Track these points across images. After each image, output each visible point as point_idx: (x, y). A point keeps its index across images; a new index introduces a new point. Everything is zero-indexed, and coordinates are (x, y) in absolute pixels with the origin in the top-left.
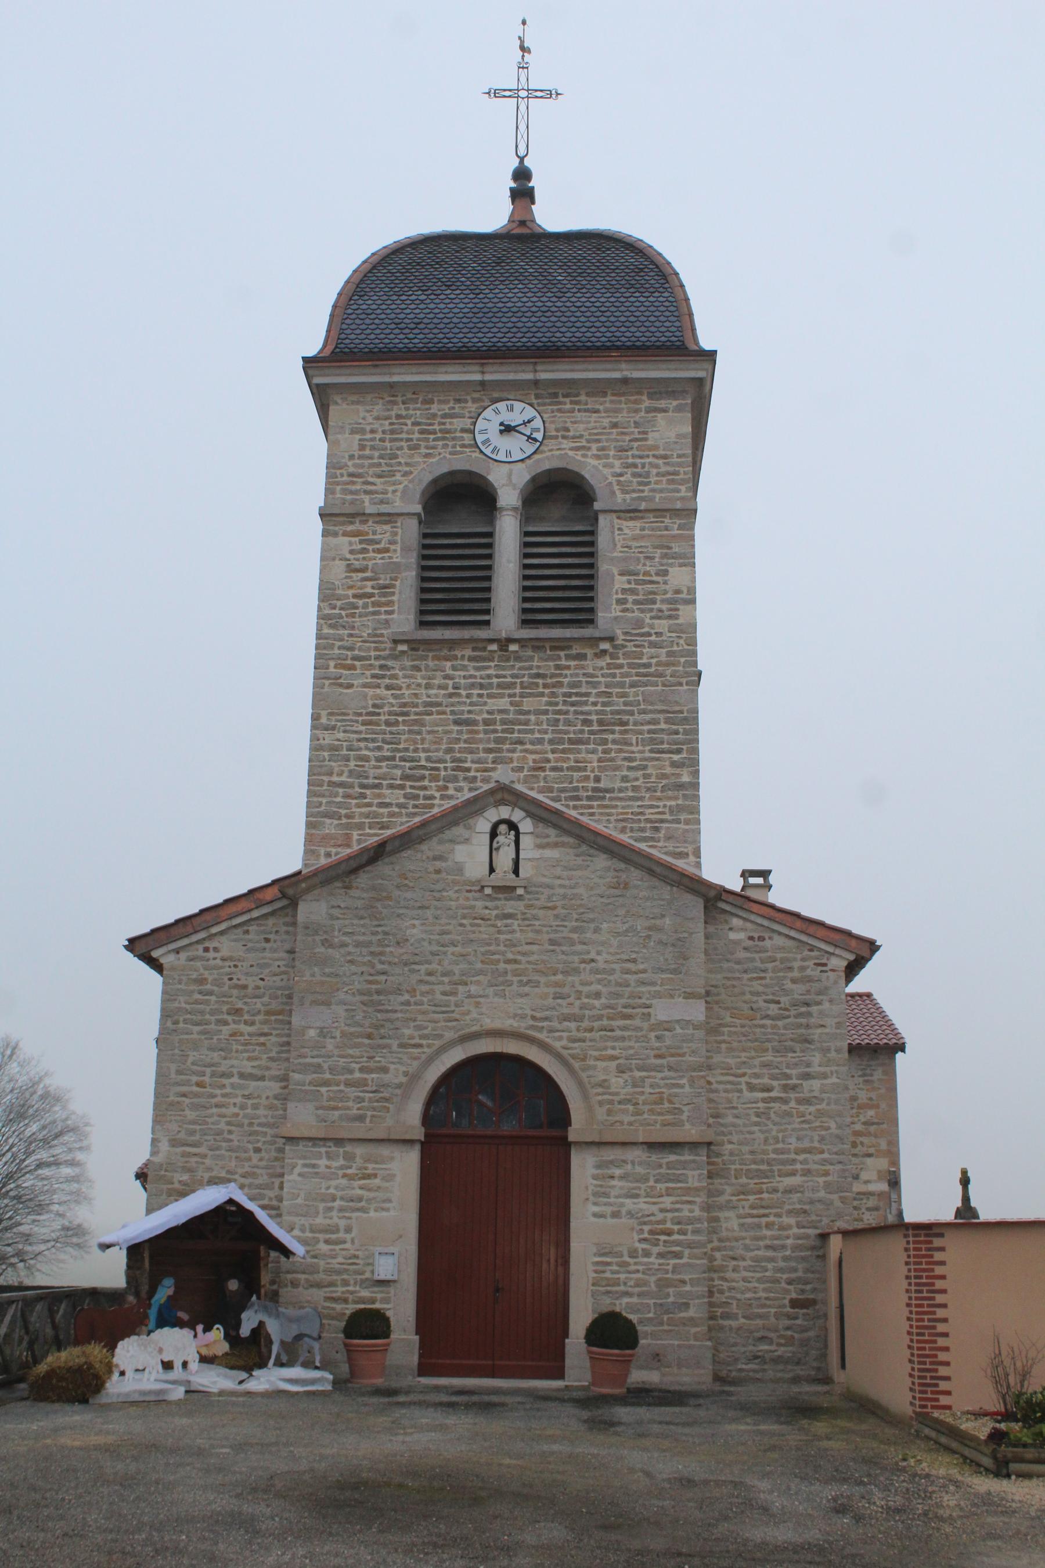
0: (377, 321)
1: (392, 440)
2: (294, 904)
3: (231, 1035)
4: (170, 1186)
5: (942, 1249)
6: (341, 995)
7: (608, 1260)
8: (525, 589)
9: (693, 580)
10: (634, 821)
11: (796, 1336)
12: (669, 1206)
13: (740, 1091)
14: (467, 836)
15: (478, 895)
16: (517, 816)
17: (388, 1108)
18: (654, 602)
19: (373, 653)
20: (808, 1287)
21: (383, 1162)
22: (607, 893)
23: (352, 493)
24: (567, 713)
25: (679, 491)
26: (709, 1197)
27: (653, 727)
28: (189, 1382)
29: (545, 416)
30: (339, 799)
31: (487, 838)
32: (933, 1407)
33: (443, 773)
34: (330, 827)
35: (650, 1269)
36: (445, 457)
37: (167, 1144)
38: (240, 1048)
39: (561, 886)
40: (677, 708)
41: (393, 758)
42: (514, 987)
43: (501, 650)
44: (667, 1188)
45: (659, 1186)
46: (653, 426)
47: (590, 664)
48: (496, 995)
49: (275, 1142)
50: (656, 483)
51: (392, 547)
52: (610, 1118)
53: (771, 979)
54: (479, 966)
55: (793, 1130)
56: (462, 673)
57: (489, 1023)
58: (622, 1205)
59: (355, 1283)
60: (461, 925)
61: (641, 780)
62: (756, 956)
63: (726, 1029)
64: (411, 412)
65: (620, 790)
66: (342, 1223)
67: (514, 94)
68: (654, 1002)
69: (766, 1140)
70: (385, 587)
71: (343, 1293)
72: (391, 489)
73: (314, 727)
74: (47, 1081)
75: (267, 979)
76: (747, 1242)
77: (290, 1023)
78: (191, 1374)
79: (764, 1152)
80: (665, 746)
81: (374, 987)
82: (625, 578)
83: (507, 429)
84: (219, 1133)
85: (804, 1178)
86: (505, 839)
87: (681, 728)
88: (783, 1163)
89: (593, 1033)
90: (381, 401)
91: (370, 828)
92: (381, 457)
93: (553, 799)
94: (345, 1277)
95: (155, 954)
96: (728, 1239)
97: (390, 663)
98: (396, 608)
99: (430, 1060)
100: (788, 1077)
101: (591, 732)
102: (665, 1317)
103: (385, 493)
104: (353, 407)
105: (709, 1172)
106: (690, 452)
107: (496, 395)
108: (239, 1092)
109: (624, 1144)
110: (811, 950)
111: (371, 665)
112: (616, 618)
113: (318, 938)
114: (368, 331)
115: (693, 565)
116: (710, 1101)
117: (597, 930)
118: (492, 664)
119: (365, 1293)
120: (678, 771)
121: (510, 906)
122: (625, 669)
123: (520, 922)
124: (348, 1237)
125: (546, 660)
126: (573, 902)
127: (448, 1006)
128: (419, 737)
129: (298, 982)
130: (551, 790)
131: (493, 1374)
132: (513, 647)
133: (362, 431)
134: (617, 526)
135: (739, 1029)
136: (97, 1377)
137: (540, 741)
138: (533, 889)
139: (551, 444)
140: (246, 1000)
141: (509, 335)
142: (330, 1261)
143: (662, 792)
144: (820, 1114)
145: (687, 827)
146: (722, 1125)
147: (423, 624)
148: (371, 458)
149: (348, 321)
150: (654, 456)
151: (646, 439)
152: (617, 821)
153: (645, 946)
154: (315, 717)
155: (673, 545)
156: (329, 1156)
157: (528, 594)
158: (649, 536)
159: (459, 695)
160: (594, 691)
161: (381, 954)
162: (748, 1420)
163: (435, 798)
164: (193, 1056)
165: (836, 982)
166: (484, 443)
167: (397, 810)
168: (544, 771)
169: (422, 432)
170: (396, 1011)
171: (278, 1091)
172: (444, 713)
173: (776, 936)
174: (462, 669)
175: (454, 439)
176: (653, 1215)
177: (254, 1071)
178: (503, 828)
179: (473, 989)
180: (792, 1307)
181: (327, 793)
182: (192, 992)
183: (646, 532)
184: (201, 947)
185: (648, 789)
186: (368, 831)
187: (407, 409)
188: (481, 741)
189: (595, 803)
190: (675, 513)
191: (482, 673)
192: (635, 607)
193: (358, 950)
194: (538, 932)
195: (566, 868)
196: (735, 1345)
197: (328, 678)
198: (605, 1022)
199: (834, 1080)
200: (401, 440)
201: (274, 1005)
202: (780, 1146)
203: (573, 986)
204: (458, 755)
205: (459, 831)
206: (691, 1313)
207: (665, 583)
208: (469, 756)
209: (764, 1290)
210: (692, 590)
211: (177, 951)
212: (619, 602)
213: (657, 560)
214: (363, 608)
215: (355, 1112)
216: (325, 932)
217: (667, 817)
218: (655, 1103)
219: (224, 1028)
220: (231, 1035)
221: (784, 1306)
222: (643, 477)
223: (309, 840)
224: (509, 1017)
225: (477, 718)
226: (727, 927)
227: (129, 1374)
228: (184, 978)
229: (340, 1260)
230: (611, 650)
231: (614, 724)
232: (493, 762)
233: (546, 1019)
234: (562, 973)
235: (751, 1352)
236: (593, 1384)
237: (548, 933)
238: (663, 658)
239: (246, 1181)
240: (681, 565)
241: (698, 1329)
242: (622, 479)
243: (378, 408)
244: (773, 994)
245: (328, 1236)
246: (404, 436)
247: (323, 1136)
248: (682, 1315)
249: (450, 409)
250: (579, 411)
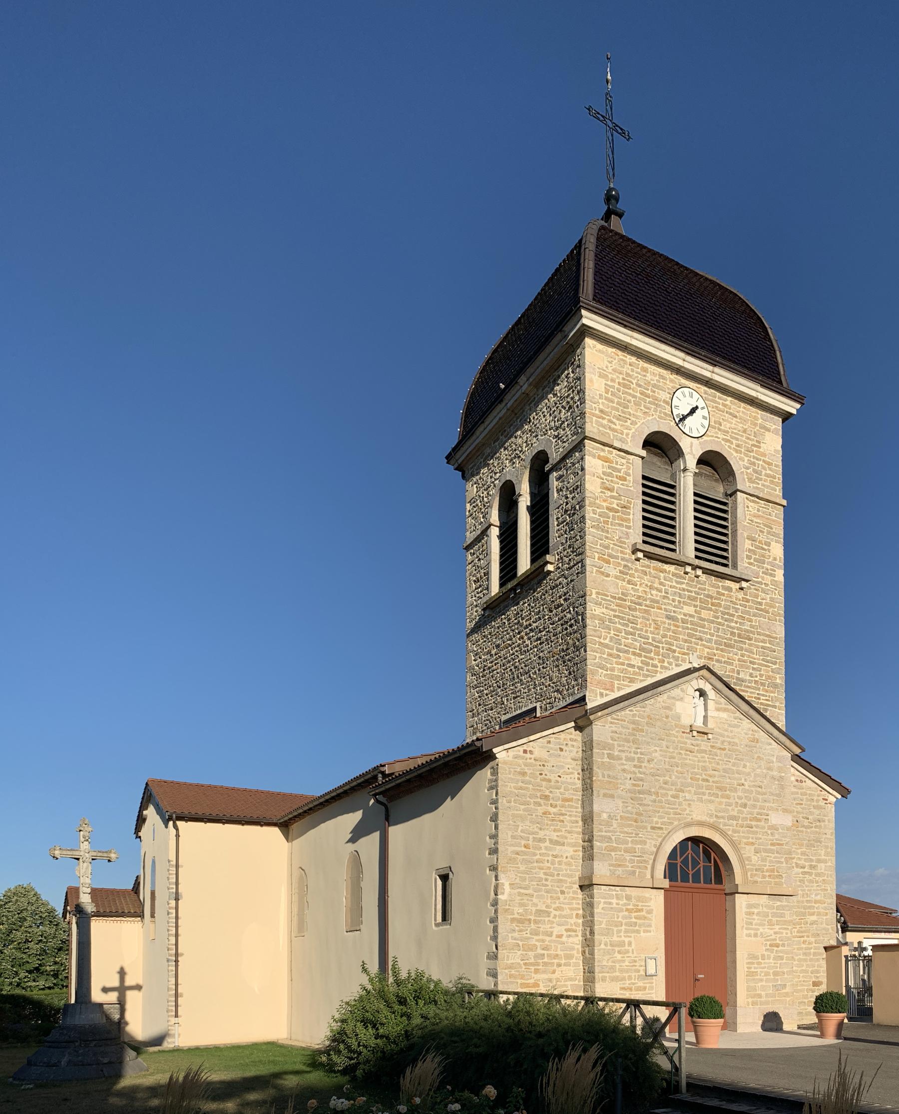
12: (777, 930)
30: (605, 656)
60: (680, 753)
84: (540, 879)
108: (551, 853)
124: (630, 949)
137: (710, 641)
156: (618, 898)
161: (640, 767)
171: (572, 853)
172: (661, 609)
179: (688, 796)
184: (521, 749)
195: (730, 725)
199: (829, 864)
205: (676, 692)
229: (627, 964)
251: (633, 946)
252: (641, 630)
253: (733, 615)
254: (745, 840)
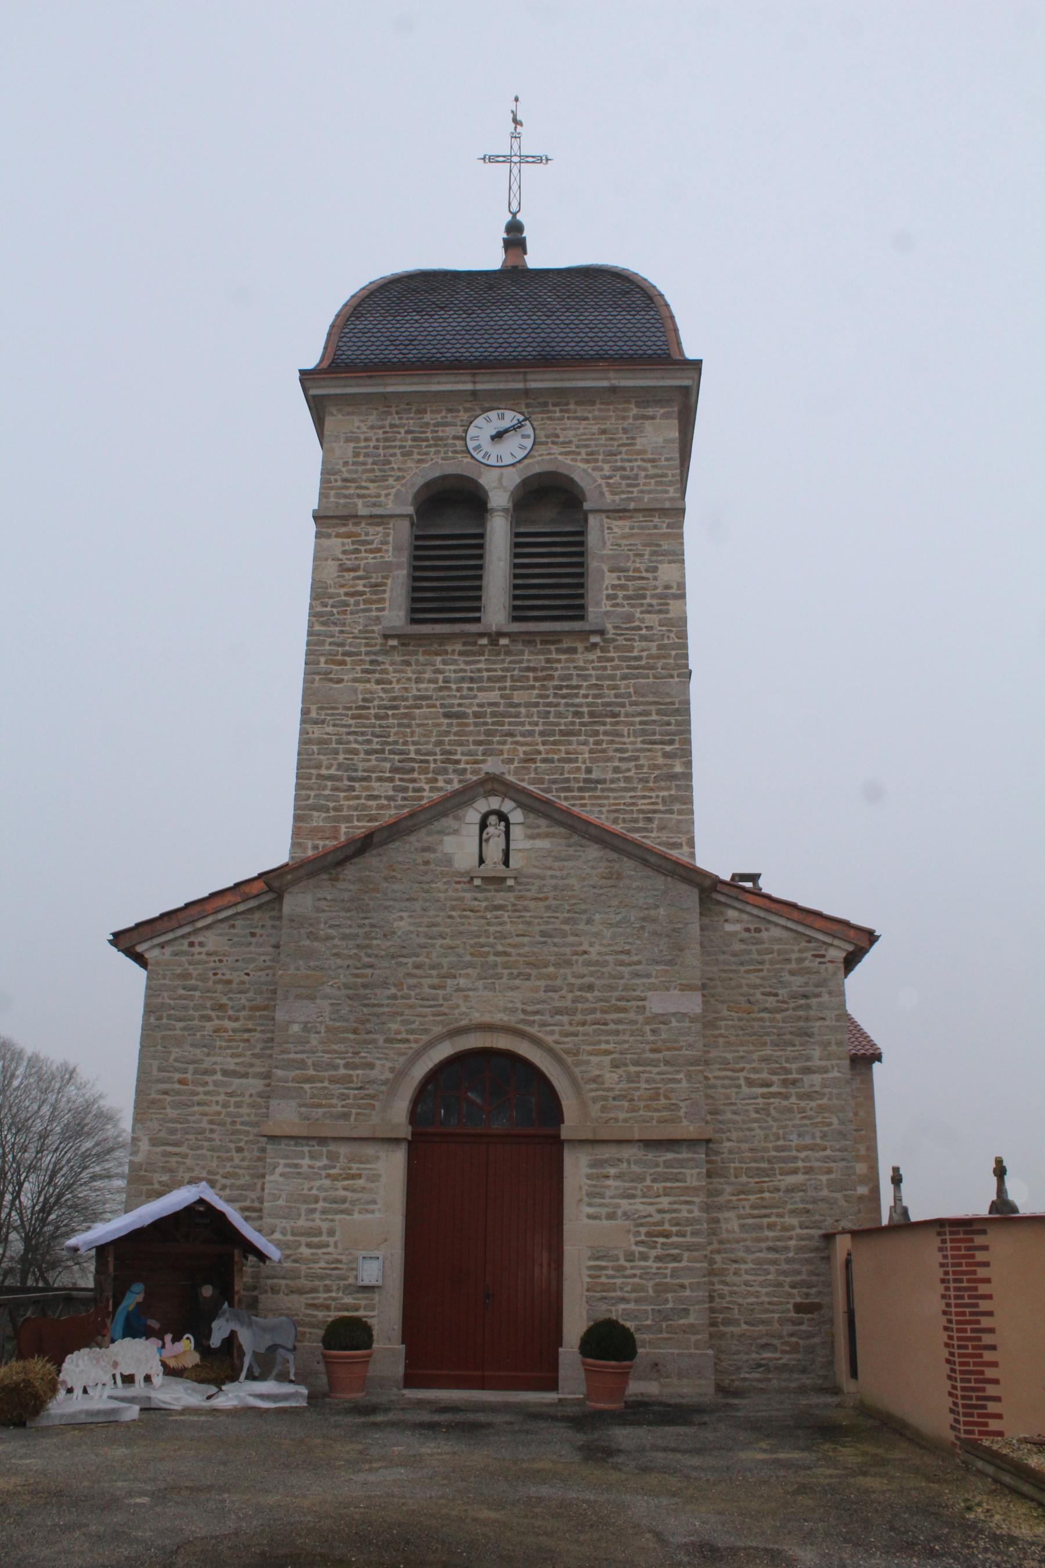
0: (373, 339)
1: (385, 448)
2: (280, 898)
3: (215, 1032)
4: (150, 1187)
5: (985, 1248)
6: (328, 990)
7: (604, 1264)
8: (516, 587)
9: (683, 576)
10: (625, 812)
11: (801, 1342)
12: (666, 1206)
13: (739, 1086)
14: (456, 827)
15: (467, 886)
16: (507, 806)
17: (374, 1106)
18: (644, 597)
19: (363, 649)
20: (813, 1290)
21: (368, 1162)
22: (600, 883)
23: (346, 497)
24: (557, 705)
25: (667, 492)
26: (708, 1197)
27: (645, 719)
28: (149, 1398)
29: (535, 423)
30: (327, 792)
31: (476, 829)
32: (981, 1433)
33: (432, 765)
34: (318, 819)
35: (648, 1273)
36: (437, 463)
37: (147, 1143)
38: (224, 1044)
39: (552, 877)
40: (669, 700)
41: (383, 751)
42: (504, 980)
43: (491, 645)
44: (665, 1188)
45: (656, 1185)
46: (642, 432)
47: (580, 658)
48: (485, 988)
49: (258, 1142)
50: (645, 484)
51: (384, 547)
52: (604, 1115)
53: (768, 970)
54: (468, 958)
55: (794, 1126)
56: (452, 667)
57: (477, 1017)
58: (618, 1206)
59: (338, 1289)
60: (450, 917)
61: (633, 771)
62: (754, 948)
63: (723, 1023)
64: (404, 421)
65: (612, 781)
66: (325, 1226)
67: (507, 159)
68: (649, 994)
69: (766, 1137)
70: (377, 585)
71: (325, 1299)
72: (383, 493)
73: (303, 721)
74: (102, 1103)
75: (252, 973)
76: (748, 1243)
77: (273, 1019)
78: (154, 1389)
79: (766, 1150)
80: (657, 737)
81: (360, 980)
82: (615, 575)
83: (498, 436)
84: (202, 1132)
85: (807, 1177)
86: (495, 829)
87: (672, 719)
88: (784, 1160)
89: (586, 1027)
90: (375, 412)
91: (358, 821)
92: (374, 463)
93: (543, 790)
94: (327, 1282)
95: (139, 949)
96: (729, 1241)
97: (380, 659)
98: (387, 605)
99: (418, 1054)
100: (788, 1071)
101: (582, 724)
102: (664, 1325)
103: (378, 496)
104: (349, 417)
105: (708, 1171)
106: (677, 455)
107: (487, 405)
109: (619, 1142)
110: (809, 942)
111: (361, 660)
112: (606, 613)
113: (303, 931)
114: (364, 348)
115: (683, 561)
116: (708, 1097)
117: (589, 922)
118: (482, 658)
119: (348, 1300)
120: (669, 762)
121: (500, 898)
122: (616, 662)
123: (510, 913)
124: (331, 1240)
125: (536, 654)
126: (565, 892)
127: (437, 1000)
128: (408, 730)
129: (282, 975)
130: (541, 781)
131: (482, 1384)
132: (504, 641)
133: (357, 440)
134: (606, 526)
135: (736, 1022)
136: (36, 1396)
137: (531, 733)
138: (525, 880)
139: (541, 449)
140: (230, 995)
141: (501, 350)
142: (311, 1265)
143: (654, 782)
144: (821, 1109)
145: (680, 817)
146: (721, 1122)
147: (414, 621)
148: (364, 464)
149: (345, 339)
150: (643, 460)
151: (634, 444)
152: (609, 811)
153: (638, 938)
154: (305, 712)
155: (662, 543)
156: (312, 1157)
157: (518, 592)
158: (639, 534)
159: (449, 689)
160: (585, 684)
161: (367, 946)
162: (763, 1445)
163: (424, 790)
164: (176, 1052)
165: (835, 974)
166: (475, 449)
167: (386, 802)
168: (535, 762)
169: (414, 440)
170: (382, 1005)
171: (261, 1088)
172: (434, 706)
173: (773, 928)
174: (452, 665)
175: (445, 445)
176: (650, 1216)
177: (237, 1068)
178: (493, 819)
179: (462, 982)
180: (797, 1312)
181: (316, 786)
182: (177, 987)
183: (636, 531)
184: (186, 942)
185: (641, 780)
186: (356, 823)
187: (400, 419)
188: (470, 733)
189: (587, 794)
190: (664, 512)
191: (472, 667)
192: (625, 602)
193: (344, 943)
194: (529, 923)
195: (556, 859)
196: (738, 1352)
197: (319, 674)
198: (598, 1015)
199: (835, 1074)
200: (395, 447)
201: (259, 1001)
202: (781, 1143)
203: (565, 979)
204: (448, 748)
205: (448, 822)
206: (692, 1319)
207: (655, 579)
208: (459, 748)
209: (767, 1294)
210: (682, 586)
211: (162, 946)
212: (609, 597)
213: (646, 557)
214: (355, 605)
215: (340, 1109)
216: (311, 925)
217: (660, 807)
218: (651, 1099)
219: (208, 1024)
220: (215, 1032)
221: (788, 1311)
222: (632, 480)
223: (297, 833)
224: (499, 1011)
225: (468, 711)
226: (722, 919)
227: (78, 1391)
228: (168, 973)
229: (323, 1264)
230: (602, 644)
231: (606, 716)
232: (484, 754)
233: (537, 1012)
234: (553, 965)
235: (754, 1360)
236: (588, 1397)
237: (539, 924)
238: (654, 651)
239: (228, 1182)
240: (670, 562)
241: (699, 1337)
242: (611, 481)
243: (373, 419)
244: (770, 987)
245: (309, 1240)
246: (398, 443)
247: (305, 1134)
248: (682, 1321)
249: (442, 418)
250: (569, 418)
251: (338, 1234)
252: (396, 743)
253: (579, 687)
254: (590, 1048)
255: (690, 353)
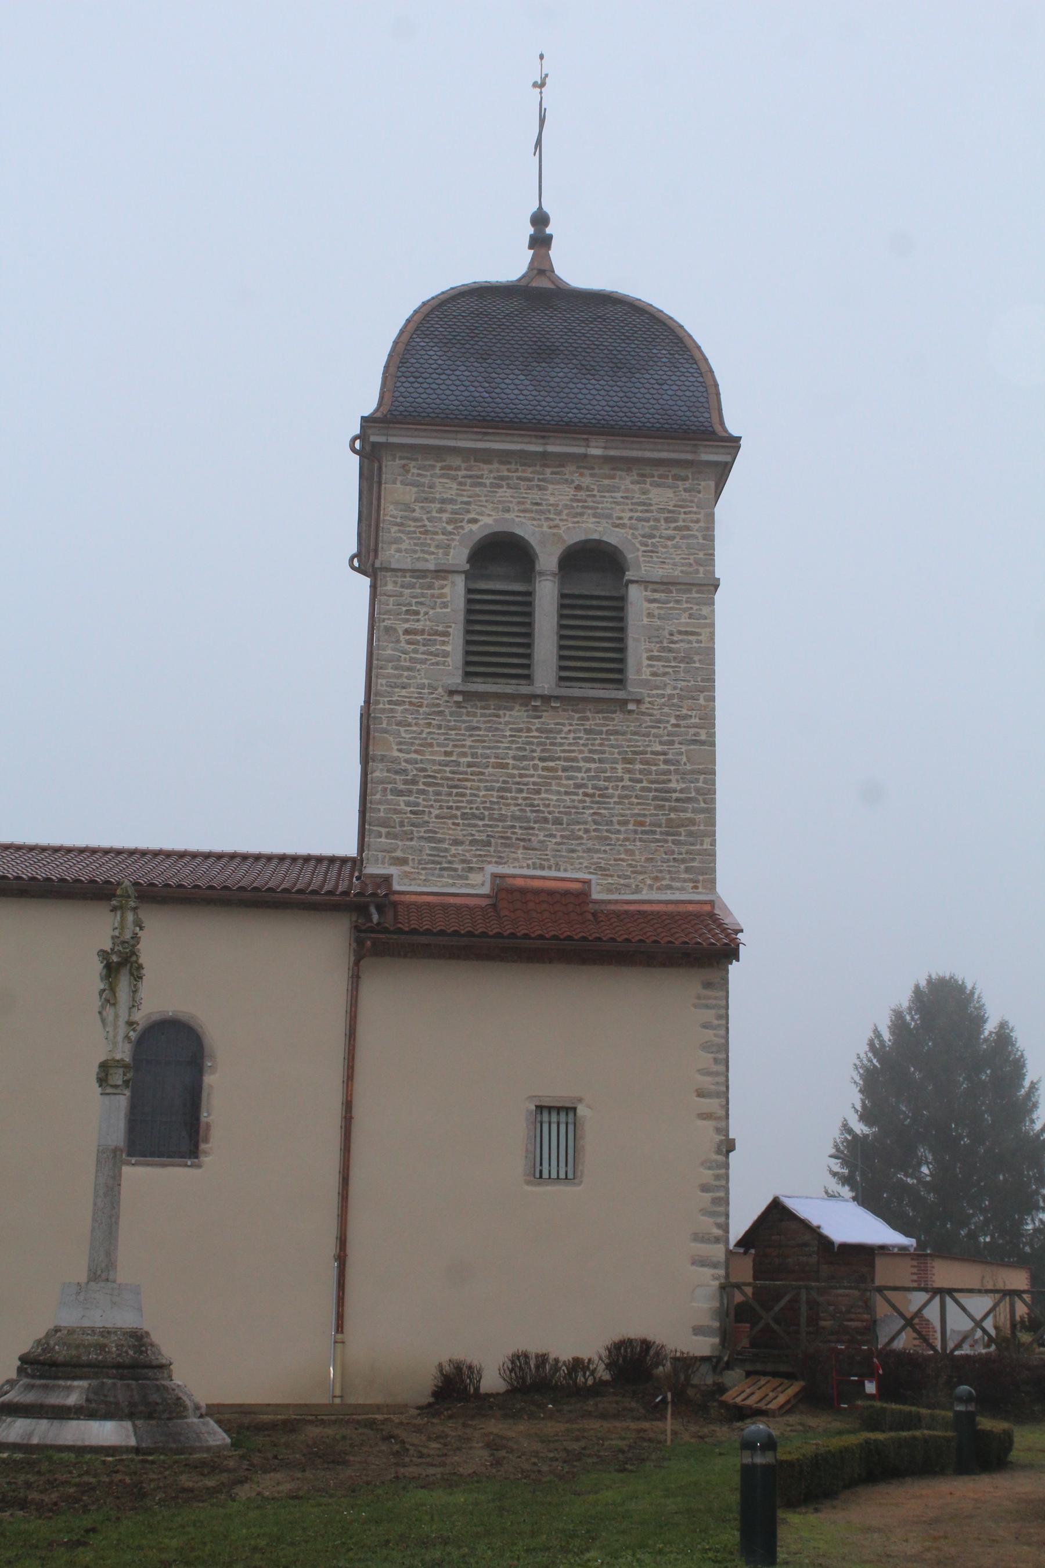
255: (733, 429)
